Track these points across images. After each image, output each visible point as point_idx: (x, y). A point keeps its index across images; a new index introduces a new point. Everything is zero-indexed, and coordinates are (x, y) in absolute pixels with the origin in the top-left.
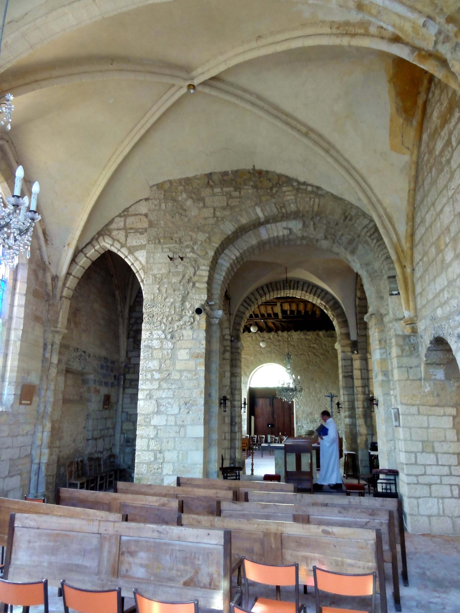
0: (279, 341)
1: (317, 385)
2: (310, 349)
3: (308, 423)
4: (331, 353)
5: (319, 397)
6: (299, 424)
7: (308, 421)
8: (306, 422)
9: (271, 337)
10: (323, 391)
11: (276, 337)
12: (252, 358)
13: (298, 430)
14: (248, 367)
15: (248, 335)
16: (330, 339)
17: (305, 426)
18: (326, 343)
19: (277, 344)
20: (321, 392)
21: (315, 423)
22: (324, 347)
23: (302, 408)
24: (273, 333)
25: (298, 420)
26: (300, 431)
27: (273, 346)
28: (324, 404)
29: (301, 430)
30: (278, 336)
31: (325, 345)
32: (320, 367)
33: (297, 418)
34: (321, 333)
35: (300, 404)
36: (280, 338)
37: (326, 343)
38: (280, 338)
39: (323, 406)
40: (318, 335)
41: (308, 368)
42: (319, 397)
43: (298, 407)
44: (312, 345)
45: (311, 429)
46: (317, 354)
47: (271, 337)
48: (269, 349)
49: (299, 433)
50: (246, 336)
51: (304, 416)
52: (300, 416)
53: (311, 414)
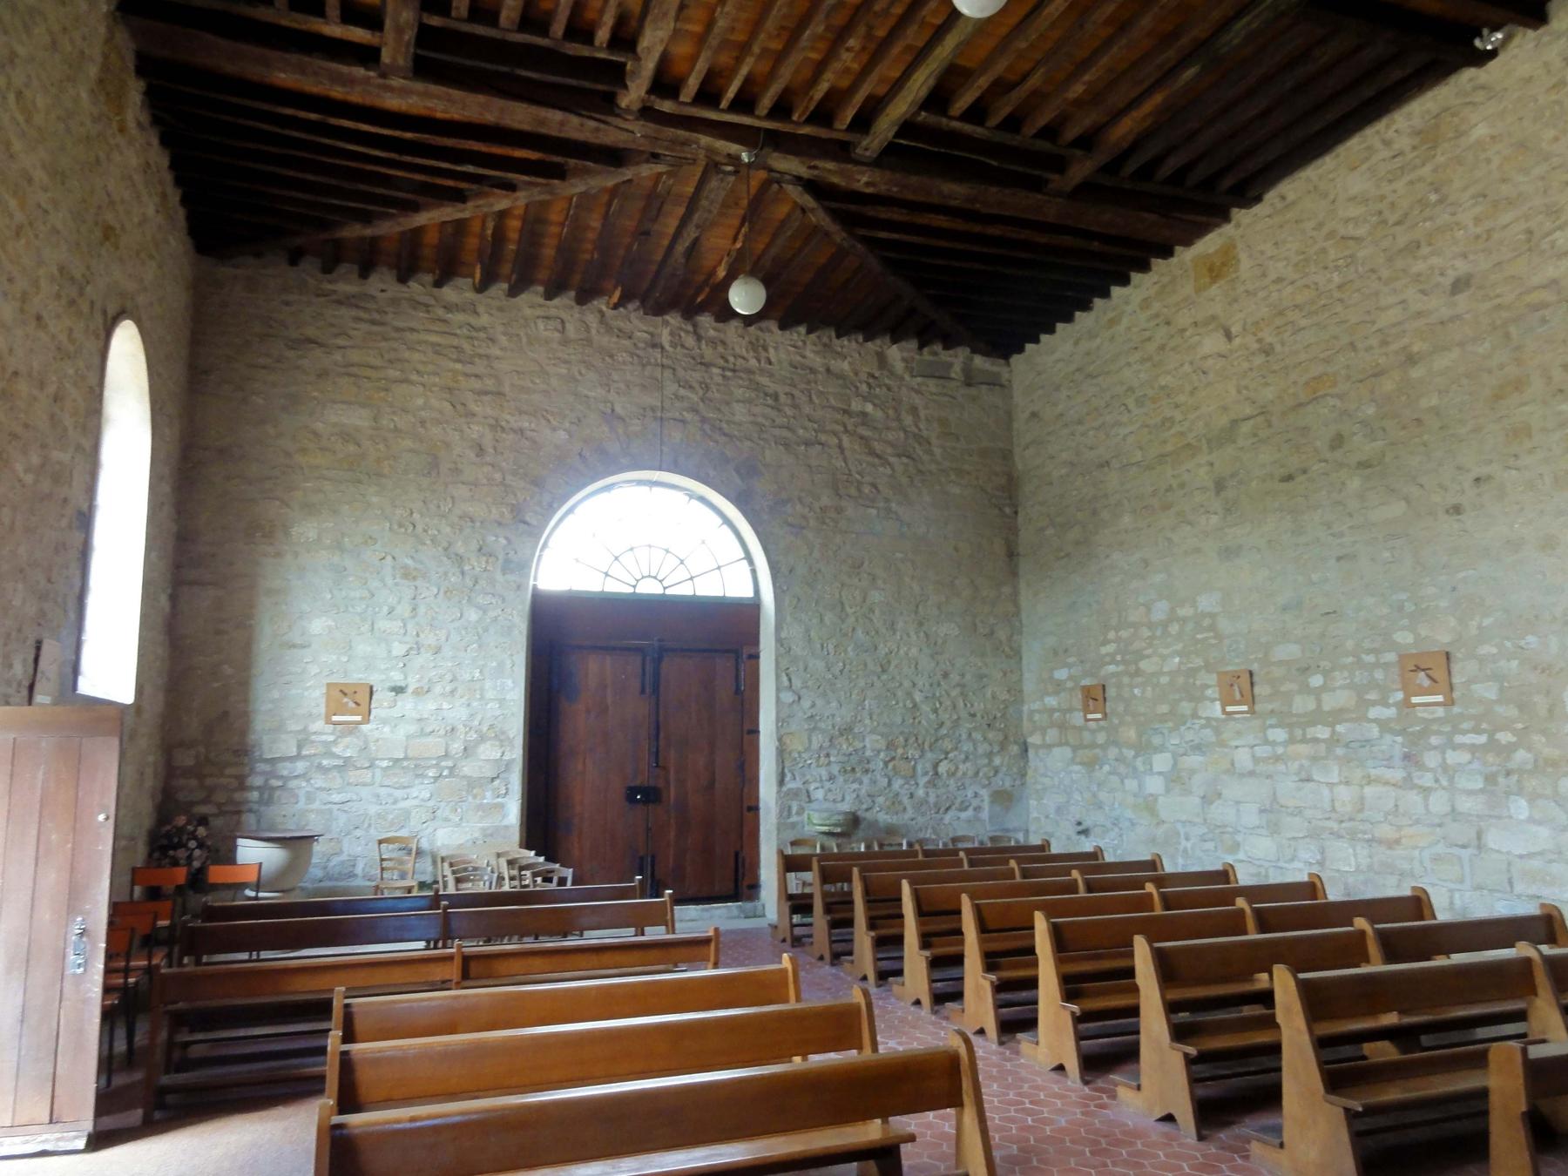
0: (707, 365)
1: (876, 596)
2: (850, 422)
3: (832, 778)
4: (937, 451)
5: (882, 650)
6: (790, 785)
7: (835, 769)
8: (824, 772)
9: (665, 339)
10: (900, 625)
11: (690, 341)
12: (562, 435)
13: (785, 811)
14: (537, 482)
15: (539, 312)
16: (931, 383)
17: (819, 794)
18: (917, 400)
19: (695, 376)
20: (892, 627)
21: (866, 780)
22: (908, 420)
23: (806, 704)
24: (674, 319)
25: (787, 764)
26: (794, 819)
27: (671, 388)
28: (907, 684)
29: (800, 811)
30: (699, 338)
31: (914, 410)
32: (888, 510)
33: (781, 753)
34: (896, 353)
35: (797, 683)
36: (708, 353)
37: (917, 400)
38: (708, 353)
39: (899, 693)
40: (882, 360)
41: (839, 510)
42: (882, 650)
43: (788, 697)
44: (856, 405)
45: (846, 807)
46: (877, 446)
47: (665, 339)
48: (651, 400)
49: (793, 825)
50: (528, 312)
51: (815, 745)
52: (796, 745)
53: (846, 731)
